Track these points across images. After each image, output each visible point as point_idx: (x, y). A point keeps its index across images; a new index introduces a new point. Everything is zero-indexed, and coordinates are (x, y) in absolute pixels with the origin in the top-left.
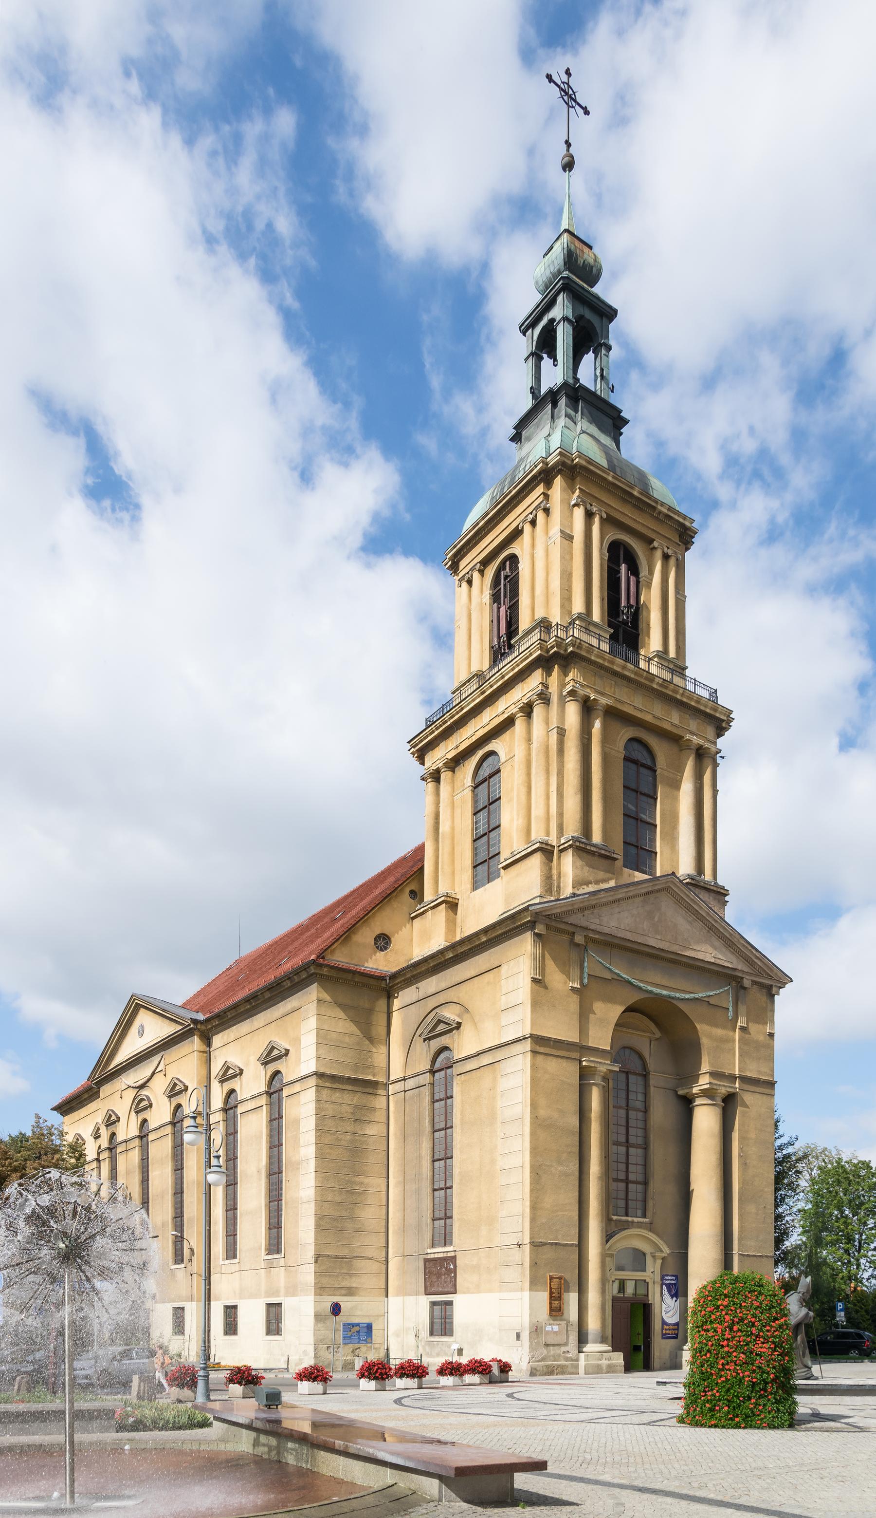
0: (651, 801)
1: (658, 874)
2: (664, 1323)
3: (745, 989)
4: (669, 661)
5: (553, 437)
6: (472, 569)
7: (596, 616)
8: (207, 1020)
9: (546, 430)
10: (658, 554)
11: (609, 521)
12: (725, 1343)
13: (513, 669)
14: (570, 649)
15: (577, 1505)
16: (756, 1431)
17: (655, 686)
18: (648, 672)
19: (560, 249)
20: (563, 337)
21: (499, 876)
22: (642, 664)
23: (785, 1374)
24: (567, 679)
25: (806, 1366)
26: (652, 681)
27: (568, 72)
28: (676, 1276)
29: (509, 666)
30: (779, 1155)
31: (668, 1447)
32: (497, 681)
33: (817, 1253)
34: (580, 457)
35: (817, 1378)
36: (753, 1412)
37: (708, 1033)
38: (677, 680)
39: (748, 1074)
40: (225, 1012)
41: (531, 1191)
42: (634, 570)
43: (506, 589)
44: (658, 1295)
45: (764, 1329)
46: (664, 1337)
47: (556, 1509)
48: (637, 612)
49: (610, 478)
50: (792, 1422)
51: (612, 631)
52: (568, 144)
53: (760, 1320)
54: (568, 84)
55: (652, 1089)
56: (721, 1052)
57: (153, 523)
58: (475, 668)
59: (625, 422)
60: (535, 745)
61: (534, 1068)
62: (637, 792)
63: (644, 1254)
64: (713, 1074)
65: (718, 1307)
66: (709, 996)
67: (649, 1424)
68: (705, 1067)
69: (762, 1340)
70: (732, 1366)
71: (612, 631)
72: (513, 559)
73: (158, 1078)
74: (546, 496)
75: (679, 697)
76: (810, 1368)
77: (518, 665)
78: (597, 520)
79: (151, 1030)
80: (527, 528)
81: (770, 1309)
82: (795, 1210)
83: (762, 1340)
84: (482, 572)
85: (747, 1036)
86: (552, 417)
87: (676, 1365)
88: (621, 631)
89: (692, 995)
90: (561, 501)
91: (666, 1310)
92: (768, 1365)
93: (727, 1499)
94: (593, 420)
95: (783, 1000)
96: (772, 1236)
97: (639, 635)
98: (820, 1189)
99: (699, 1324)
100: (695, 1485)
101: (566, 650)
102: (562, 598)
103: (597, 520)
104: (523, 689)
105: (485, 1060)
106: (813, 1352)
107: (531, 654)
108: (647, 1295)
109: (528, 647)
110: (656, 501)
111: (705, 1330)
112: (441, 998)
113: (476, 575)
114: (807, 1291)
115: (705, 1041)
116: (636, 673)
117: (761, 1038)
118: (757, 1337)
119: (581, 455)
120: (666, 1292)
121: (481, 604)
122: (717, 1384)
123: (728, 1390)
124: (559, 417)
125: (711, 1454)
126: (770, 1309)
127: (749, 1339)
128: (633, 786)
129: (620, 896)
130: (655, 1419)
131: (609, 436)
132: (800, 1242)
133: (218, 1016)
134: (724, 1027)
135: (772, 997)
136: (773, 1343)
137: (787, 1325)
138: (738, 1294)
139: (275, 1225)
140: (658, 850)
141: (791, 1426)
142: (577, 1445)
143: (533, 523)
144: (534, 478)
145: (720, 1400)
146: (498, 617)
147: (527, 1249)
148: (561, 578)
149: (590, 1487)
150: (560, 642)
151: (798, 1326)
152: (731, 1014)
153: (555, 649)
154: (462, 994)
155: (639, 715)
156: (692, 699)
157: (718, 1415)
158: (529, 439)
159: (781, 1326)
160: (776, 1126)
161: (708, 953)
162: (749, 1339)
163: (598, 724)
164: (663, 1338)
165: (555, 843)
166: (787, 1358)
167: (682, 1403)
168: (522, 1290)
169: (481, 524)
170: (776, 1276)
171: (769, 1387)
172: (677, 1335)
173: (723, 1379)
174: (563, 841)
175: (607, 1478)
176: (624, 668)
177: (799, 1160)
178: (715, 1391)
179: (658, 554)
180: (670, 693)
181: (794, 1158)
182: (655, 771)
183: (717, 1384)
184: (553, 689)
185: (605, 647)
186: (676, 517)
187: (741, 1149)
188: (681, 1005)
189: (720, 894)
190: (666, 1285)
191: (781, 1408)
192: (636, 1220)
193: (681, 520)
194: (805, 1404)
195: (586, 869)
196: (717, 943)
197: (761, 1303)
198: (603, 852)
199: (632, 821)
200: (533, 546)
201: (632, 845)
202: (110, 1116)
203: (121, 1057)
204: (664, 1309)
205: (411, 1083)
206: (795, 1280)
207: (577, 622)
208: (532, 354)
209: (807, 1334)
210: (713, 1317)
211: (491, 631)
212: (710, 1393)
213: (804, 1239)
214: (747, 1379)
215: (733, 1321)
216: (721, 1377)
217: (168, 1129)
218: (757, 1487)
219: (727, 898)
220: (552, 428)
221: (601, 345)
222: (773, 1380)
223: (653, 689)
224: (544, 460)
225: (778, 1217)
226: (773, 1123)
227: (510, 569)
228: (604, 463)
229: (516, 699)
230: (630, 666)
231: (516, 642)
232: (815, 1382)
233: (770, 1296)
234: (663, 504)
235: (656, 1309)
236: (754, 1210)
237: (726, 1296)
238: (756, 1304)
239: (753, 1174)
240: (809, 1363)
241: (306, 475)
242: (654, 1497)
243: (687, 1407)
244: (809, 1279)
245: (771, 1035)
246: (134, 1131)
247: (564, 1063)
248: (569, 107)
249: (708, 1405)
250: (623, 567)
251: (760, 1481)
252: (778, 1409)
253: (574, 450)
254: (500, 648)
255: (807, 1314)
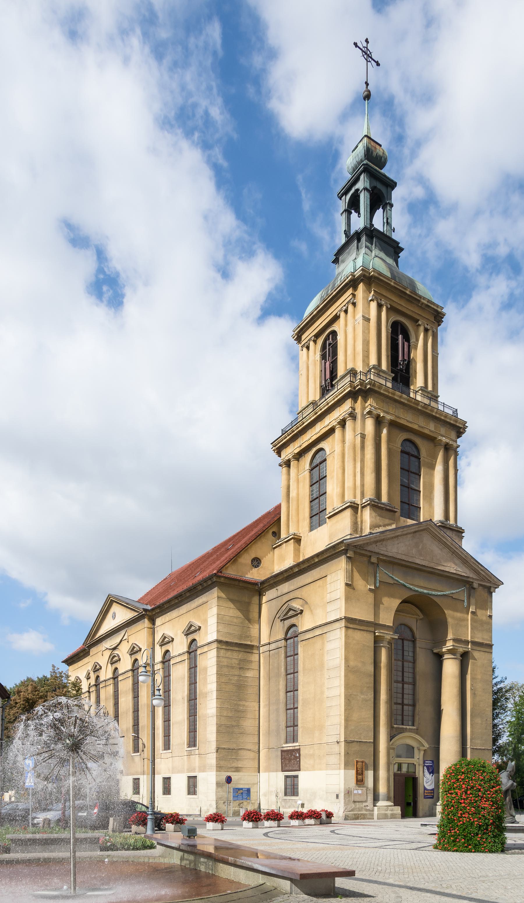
0: (417, 476)
1: (422, 520)
2: (425, 789)
3: (474, 589)
4: (428, 392)
5: (355, 262)
6: (309, 340)
7: (384, 367)
8: (153, 610)
9: (354, 256)
10: (422, 329)
11: (392, 310)
12: (462, 801)
13: (334, 399)
14: (368, 386)
15: (373, 897)
16: (481, 854)
17: (420, 408)
18: (415, 399)
19: (362, 148)
20: (364, 200)
21: (326, 523)
22: (412, 395)
23: (499, 820)
24: (367, 404)
25: (512, 815)
26: (418, 405)
27: (367, 41)
28: (432, 761)
29: (332, 397)
30: (495, 688)
31: (428, 863)
32: (325, 406)
33: (518, 748)
34: (374, 271)
35: (518, 823)
36: (479, 843)
37: (451, 616)
38: (433, 404)
39: (476, 640)
40: (163, 604)
41: (345, 710)
42: (407, 338)
43: (330, 351)
44: (421, 772)
45: (486, 793)
46: (425, 797)
47: (360, 900)
48: (409, 364)
49: (392, 284)
50: (503, 849)
51: (394, 375)
52: (367, 84)
53: (484, 788)
54: (367, 48)
55: (418, 649)
56: (460, 627)
57: (131, 306)
58: (311, 399)
59: (402, 249)
60: (347, 444)
61: (346, 636)
62: (409, 471)
63: (413, 748)
64: (455, 640)
65: (458, 780)
66: (453, 593)
67: (416, 849)
68: (450, 636)
69: (485, 799)
70: (466, 815)
71: (394, 375)
72: (334, 333)
73: (124, 643)
74: (354, 295)
75: (434, 414)
76: (514, 817)
77: (337, 397)
78: (384, 309)
79: (119, 615)
80: (342, 315)
81: (490, 781)
82: (504, 721)
83: (485, 799)
84: (315, 342)
85: (476, 617)
86: (358, 248)
87: (432, 814)
88: (399, 375)
89: (442, 593)
90: (363, 298)
91: (427, 781)
92: (489, 815)
93: (464, 894)
94: (382, 249)
95: (497, 596)
96: (491, 737)
97: (410, 377)
98: (520, 709)
99: (447, 790)
100: (444, 886)
101: (366, 387)
103: (384, 309)
104: (340, 411)
105: (318, 632)
106: (516, 807)
107: (345, 390)
108: (415, 773)
109: (343, 386)
110: (420, 297)
111: (450, 794)
112: (291, 596)
113: (312, 344)
114: (513, 771)
115: (450, 620)
116: (408, 400)
117: (484, 618)
118: (482, 797)
119: (374, 270)
120: (426, 771)
121: (315, 361)
122: (457, 826)
123: (464, 830)
124: (361, 248)
125: (454, 868)
126: (490, 781)
127: (477, 799)
128: (407, 468)
129: (399, 534)
130: (420, 846)
131: (392, 258)
132: (508, 741)
133: (159, 607)
134: (461, 612)
135: (491, 594)
136: (492, 801)
137: (500, 790)
138: (470, 772)
139: (193, 730)
140: (421, 506)
141: (503, 851)
142: (373, 861)
143: (346, 311)
144: (347, 284)
145: (459, 835)
146: (325, 368)
147: (343, 744)
148: (363, 344)
149: (381, 886)
150: (362, 382)
151: (507, 791)
152: (466, 604)
153: (359, 387)
154: (304, 593)
155: (410, 425)
156: (442, 415)
157: (458, 844)
158: (343, 261)
159: (496, 792)
160: (493, 671)
161: (452, 567)
162: (477, 799)
163: (385, 431)
164: (425, 798)
165: (359, 503)
166: (500, 810)
167: (436, 837)
168: (340, 769)
169: (314, 313)
170: (494, 761)
171: (489, 828)
172: (433, 796)
173: (461, 823)
174: (364, 501)
175: (391, 881)
176: (401, 397)
177: (507, 691)
178: (456, 830)
179: (422, 329)
180: (429, 412)
181: (504, 690)
182: (420, 459)
183: (457, 826)
184: (358, 411)
185: (389, 385)
186: (432, 306)
187: (472, 685)
188: (435, 599)
189: (459, 532)
190: (427, 766)
191: (497, 841)
192: (408, 727)
193: (435, 308)
194: (511, 838)
195: (378, 518)
196: (457, 561)
197: (484, 777)
198: (388, 508)
199: (406, 489)
200: (346, 325)
201: (406, 503)
202: (96, 666)
203: (103, 631)
204: (425, 781)
205: (273, 646)
206: (506, 764)
207: (372, 370)
208: (345, 211)
209: (512, 796)
210: (455, 785)
211: (321, 377)
212: (453, 831)
213: (511, 739)
214: (476, 823)
215: (467, 788)
216: (460, 821)
217: (130, 674)
218: (482, 887)
219: (463, 535)
220: (358, 255)
221: (387, 204)
222: (492, 824)
223: (418, 409)
224: (352, 274)
225: (495, 726)
226: (491, 669)
227: (332, 340)
228: (389, 274)
229: (335, 417)
230: (404, 396)
231: (335, 383)
232: (517, 825)
233: (490, 773)
234: (424, 298)
235: (420, 781)
236: (480, 722)
237: (463, 773)
238: (481, 778)
239: (479, 700)
240: (514, 814)
241: (225, 273)
242: (419, 893)
243: (439, 840)
244: (513, 763)
245: (490, 617)
246: (110, 675)
247: (365, 634)
248: (367, 61)
249: (452, 838)
250: (400, 337)
251: (483, 884)
252: (495, 841)
253: (371, 267)
254: (326, 387)
255: (513, 784)
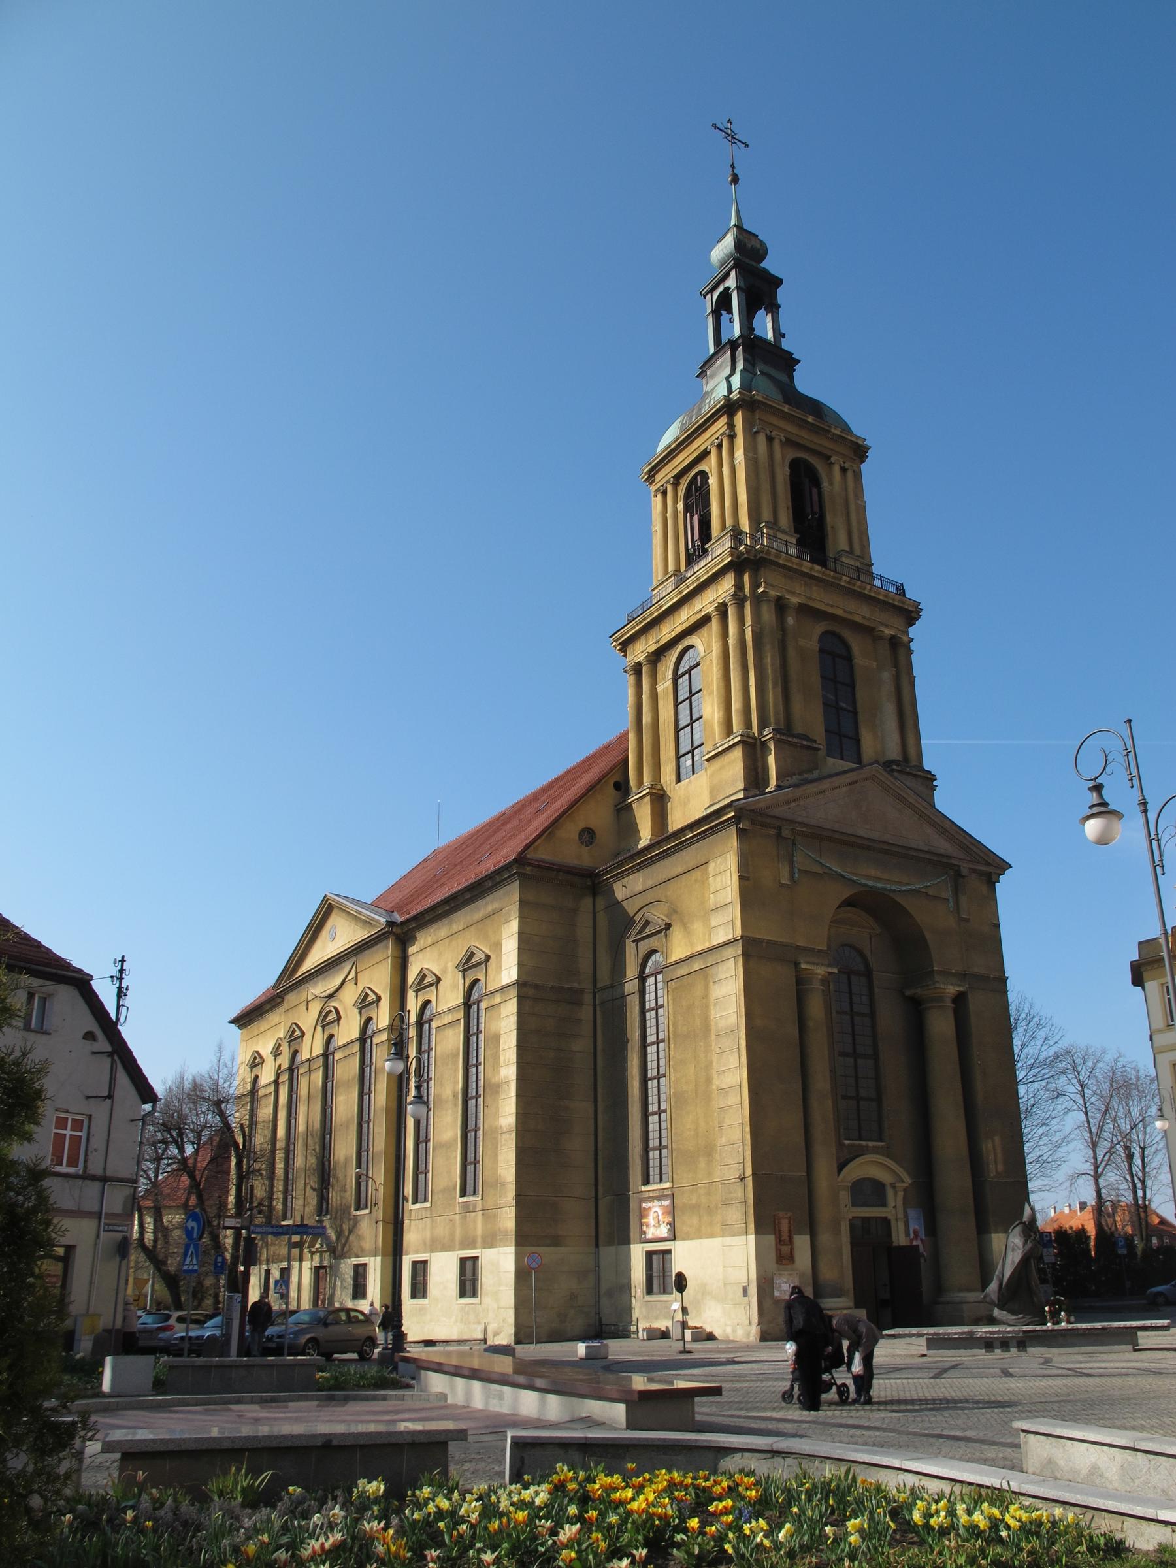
8: (403, 923)
29: (702, 569)
40: (422, 914)
55: (876, 990)
72: (704, 475)
79: (340, 936)
112: (649, 897)
133: (415, 918)
139: (468, 1162)
154: (672, 890)
155: (831, 610)
202: (294, 1031)
203: (309, 964)
246: (318, 1050)
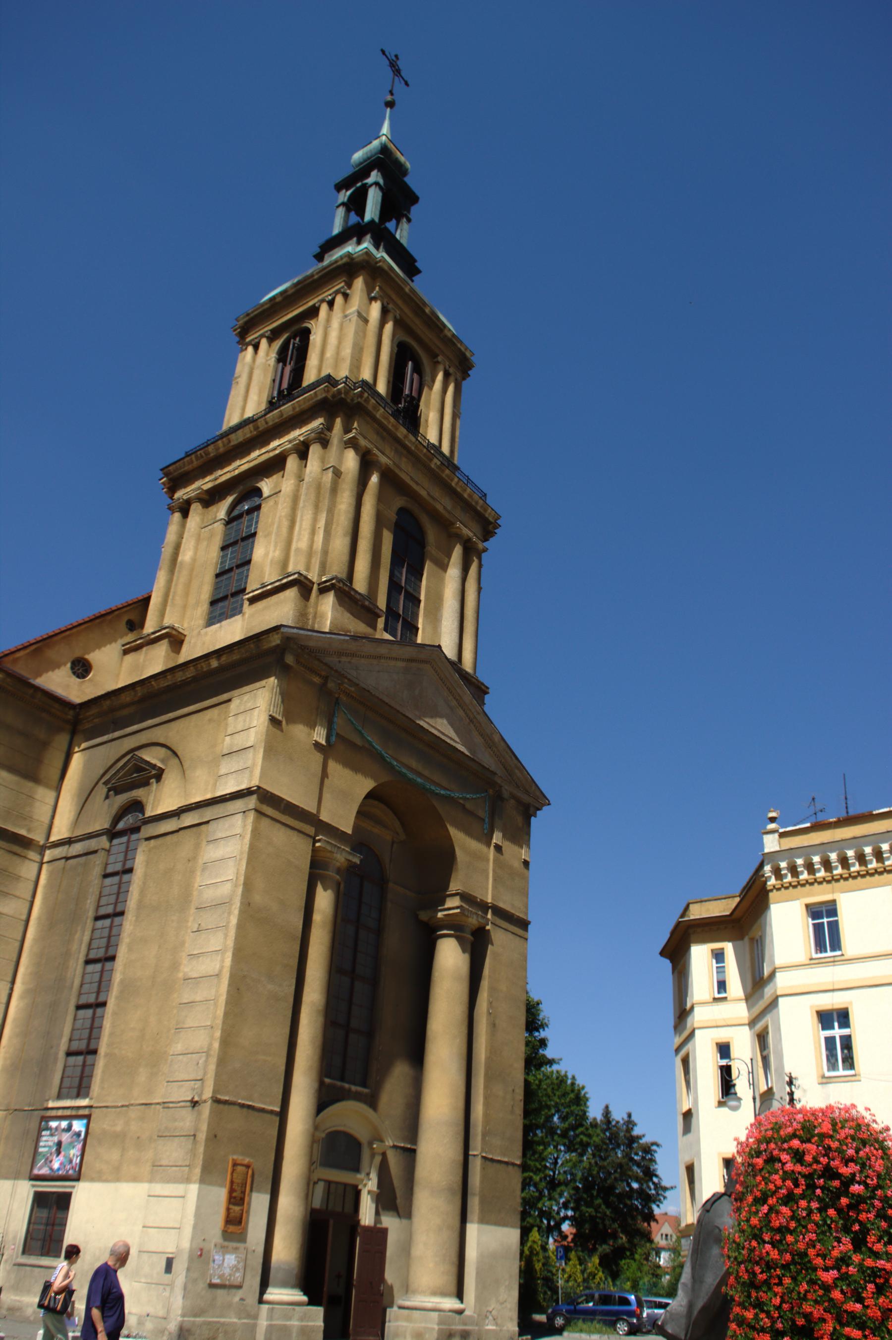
21: (240, 612)
41: (226, 1014)
61: (255, 832)
102: (352, 364)
134: (478, 839)
140: (420, 626)
147: (206, 1109)
152: (486, 826)
165: (315, 579)
168: (188, 1180)
174: (324, 579)
192: (354, 1088)
205: (77, 848)
230: (413, 439)
247: (295, 837)
